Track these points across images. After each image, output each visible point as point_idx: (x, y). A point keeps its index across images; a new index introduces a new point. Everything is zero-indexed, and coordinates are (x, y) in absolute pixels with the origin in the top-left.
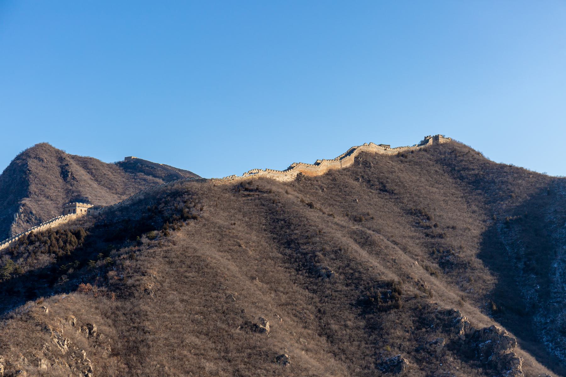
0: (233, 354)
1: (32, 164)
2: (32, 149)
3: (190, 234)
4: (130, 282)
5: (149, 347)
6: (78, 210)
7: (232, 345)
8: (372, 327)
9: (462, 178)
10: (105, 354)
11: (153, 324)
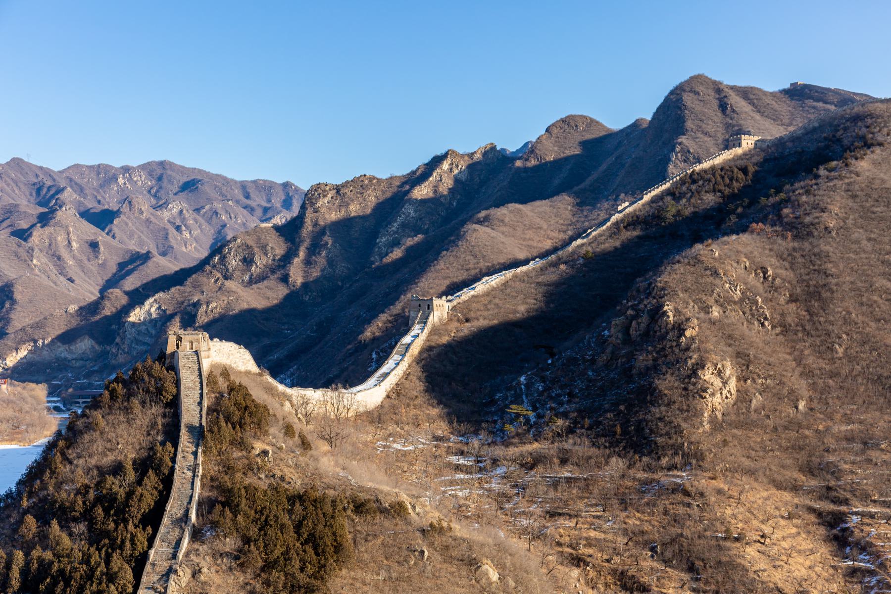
1: (688, 99)
2: (686, 82)
3: (875, 163)
4: (808, 219)
5: (833, 292)
6: (744, 143)
10: (782, 300)
11: (836, 265)
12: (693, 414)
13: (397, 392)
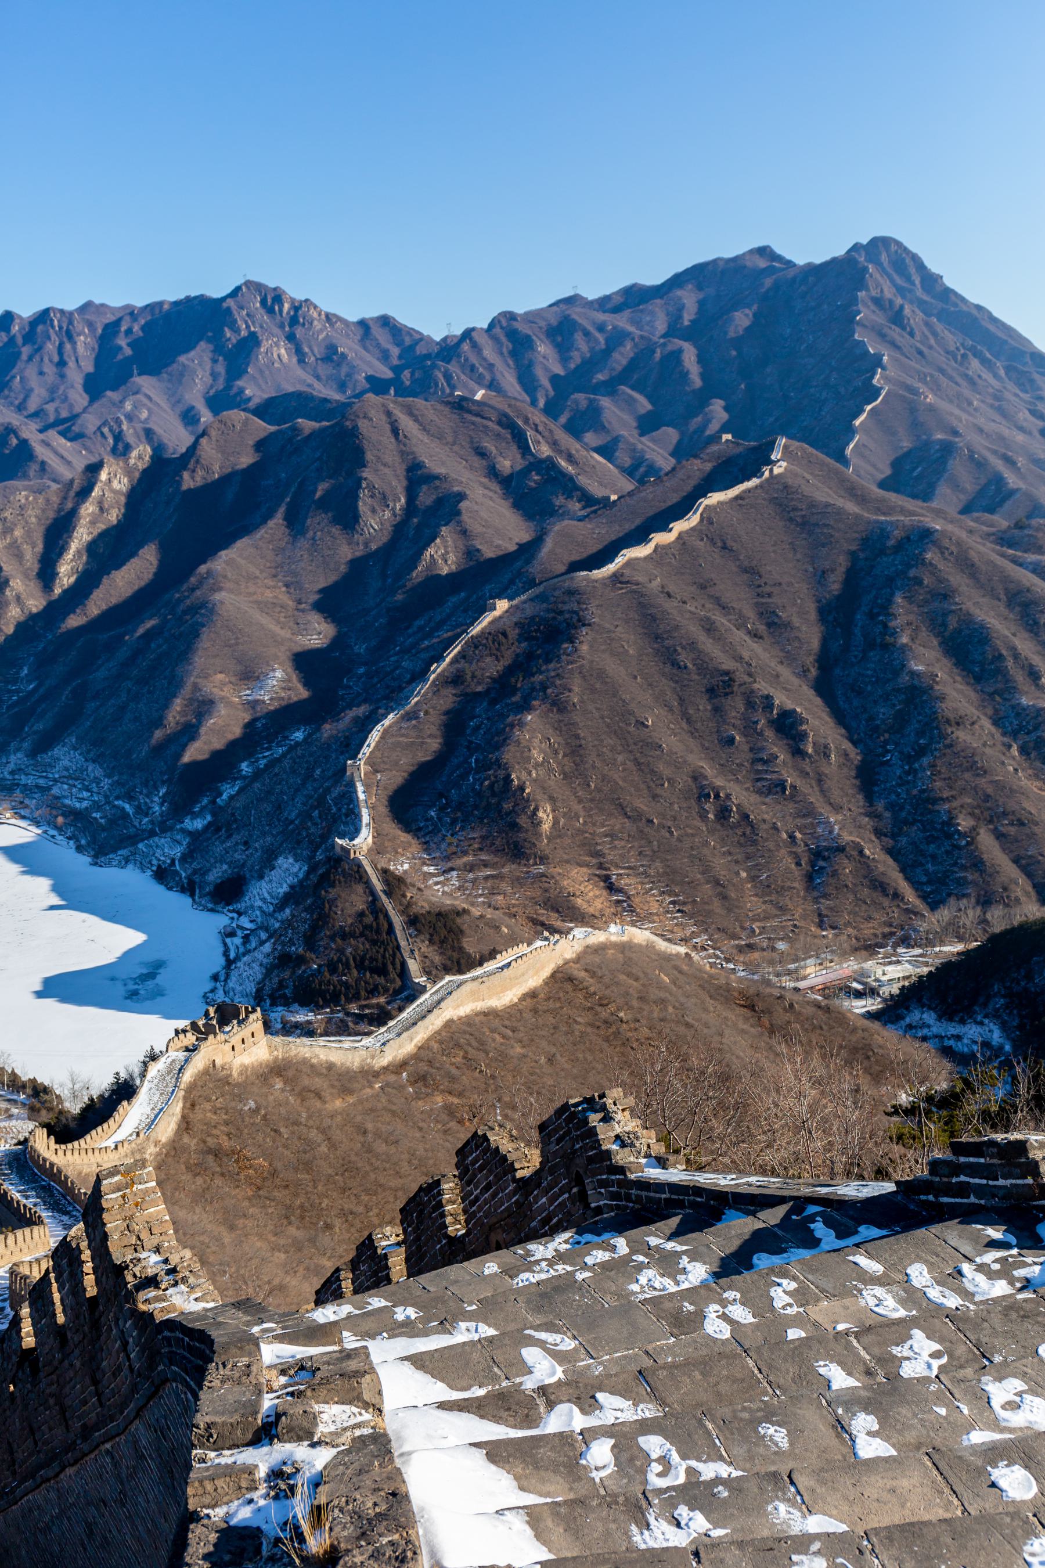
0: (632, 747)
3: (591, 647)
7: (631, 741)
8: (717, 710)
9: (791, 520)
13: (378, 835)
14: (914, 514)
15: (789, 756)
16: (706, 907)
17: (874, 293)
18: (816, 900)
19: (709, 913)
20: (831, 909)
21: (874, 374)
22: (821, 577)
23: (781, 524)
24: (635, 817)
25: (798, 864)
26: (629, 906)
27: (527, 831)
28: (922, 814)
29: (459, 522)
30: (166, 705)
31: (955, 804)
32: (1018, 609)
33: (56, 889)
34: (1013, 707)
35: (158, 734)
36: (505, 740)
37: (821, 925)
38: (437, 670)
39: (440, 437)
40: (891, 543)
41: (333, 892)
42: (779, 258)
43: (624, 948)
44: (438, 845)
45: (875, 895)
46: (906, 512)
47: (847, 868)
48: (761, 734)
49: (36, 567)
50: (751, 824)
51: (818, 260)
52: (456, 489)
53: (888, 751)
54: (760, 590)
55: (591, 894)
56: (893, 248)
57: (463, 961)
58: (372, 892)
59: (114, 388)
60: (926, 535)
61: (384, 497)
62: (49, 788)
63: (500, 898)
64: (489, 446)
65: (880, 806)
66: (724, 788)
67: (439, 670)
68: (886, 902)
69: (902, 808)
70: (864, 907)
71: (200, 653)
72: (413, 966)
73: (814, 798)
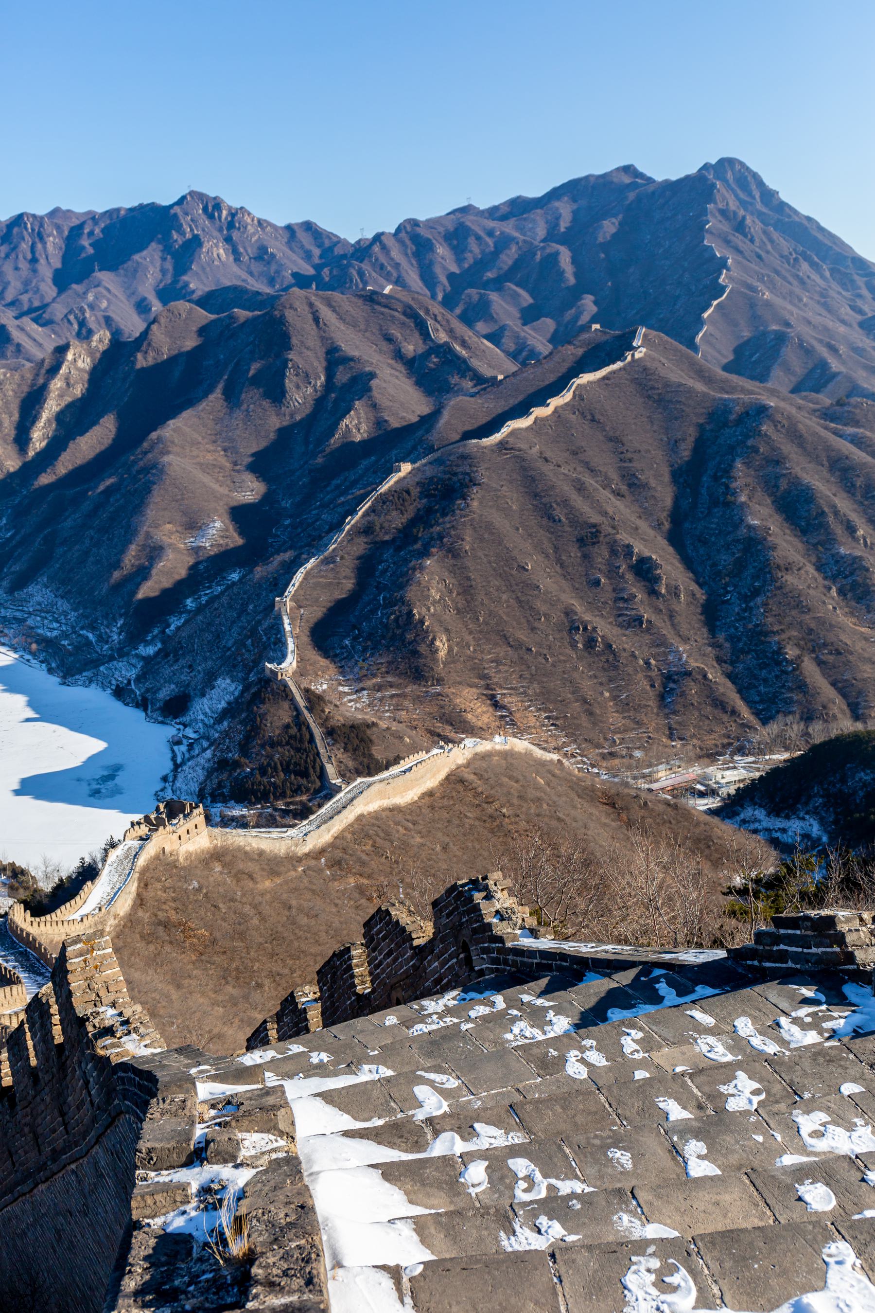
0: (515, 587)
3: (481, 503)
8: (585, 557)
9: (649, 397)
10: (454, 595)
12: (435, 660)
13: (301, 660)
14: (751, 392)
15: (646, 596)
16: (576, 721)
17: (720, 206)
18: (667, 716)
19: (578, 727)
20: (680, 723)
21: (720, 274)
22: (673, 445)
23: (641, 400)
24: (517, 646)
25: (652, 686)
26: (511, 720)
27: (426, 657)
28: (756, 645)
29: (370, 398)
30: (123, 551)
31: (783, 636)
32: (838, 473)
33: (31, 704)
34: (833, 556)
35: (117, 575)
36: (408, 581)
37: (671, 737)
38: (351, 522)
39: (354, 325)
40: (733, 417)
41: (263, 708)
42: (641, 175)
43: (507, 755)
44: (352, 668)
45: (716, 712)
46: (746, 391)
47: (693, 690)
48: (622, 577)
49: (13, 433)
50: (613, 652)
51: (674, 178)
52: (367, 369)
53: (728, 592)
54: (622, 456)
55: (479, 710)
56: (737, 167)
57: (372, 766)
58: (296, 708)
59: (79, 281)
60: (762, 410)
61: (307, 376)
62: (25, 620)
63: (404, 713)
64: (396, 333)
65: (721, 637)
66: (591, 622)
67: (353, 522)
68: (725, 718)
69: (739, 640)
70: (707, 722)
71: (151, 506)
72: (331, 769)
73: (667, 631)
